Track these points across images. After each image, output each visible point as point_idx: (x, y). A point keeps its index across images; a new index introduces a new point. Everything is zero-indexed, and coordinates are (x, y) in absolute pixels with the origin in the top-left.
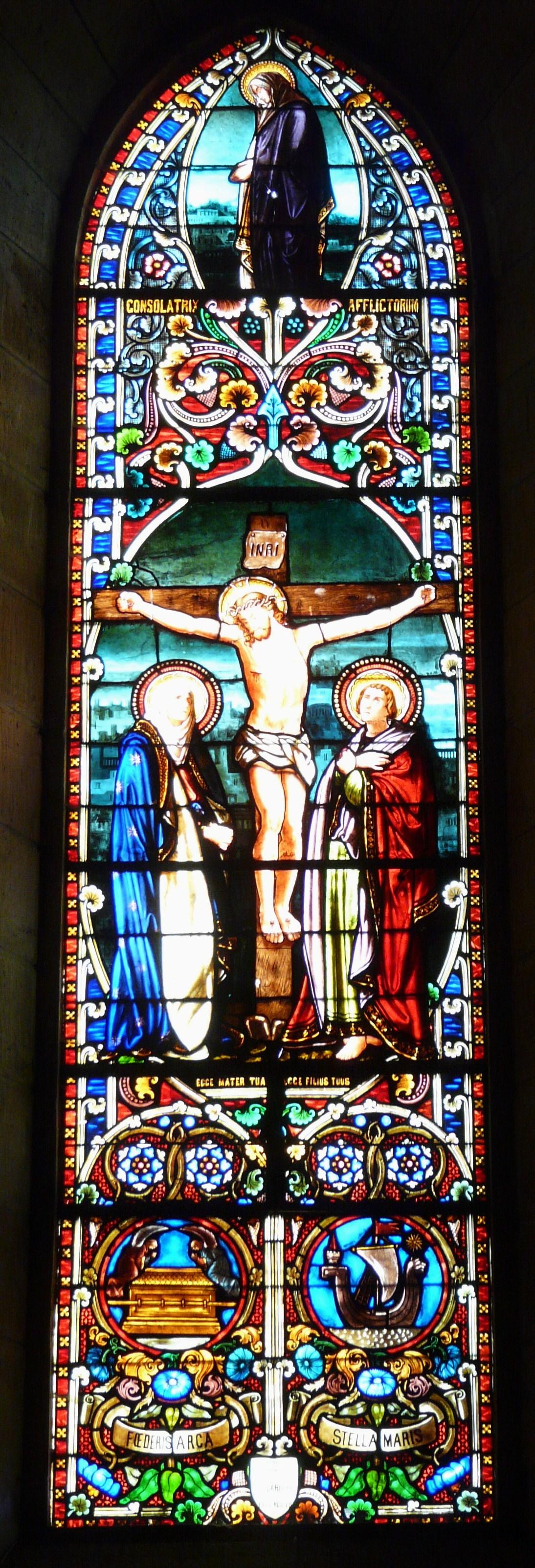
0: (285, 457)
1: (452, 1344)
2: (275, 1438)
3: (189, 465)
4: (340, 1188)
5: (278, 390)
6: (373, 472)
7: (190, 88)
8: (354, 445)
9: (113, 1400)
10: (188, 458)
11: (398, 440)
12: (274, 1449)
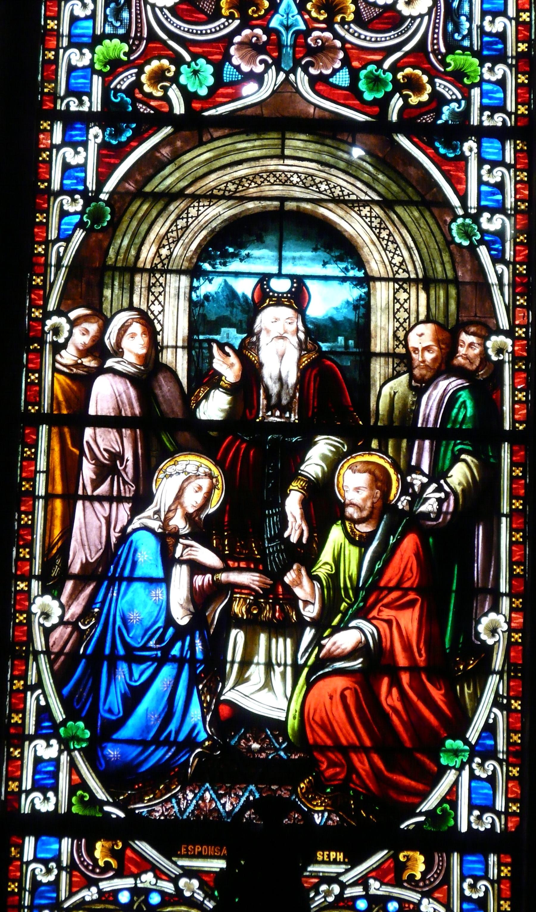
0: (301, 80)
3: (183, 89)
6: (406, 106)
10: (183, 80)
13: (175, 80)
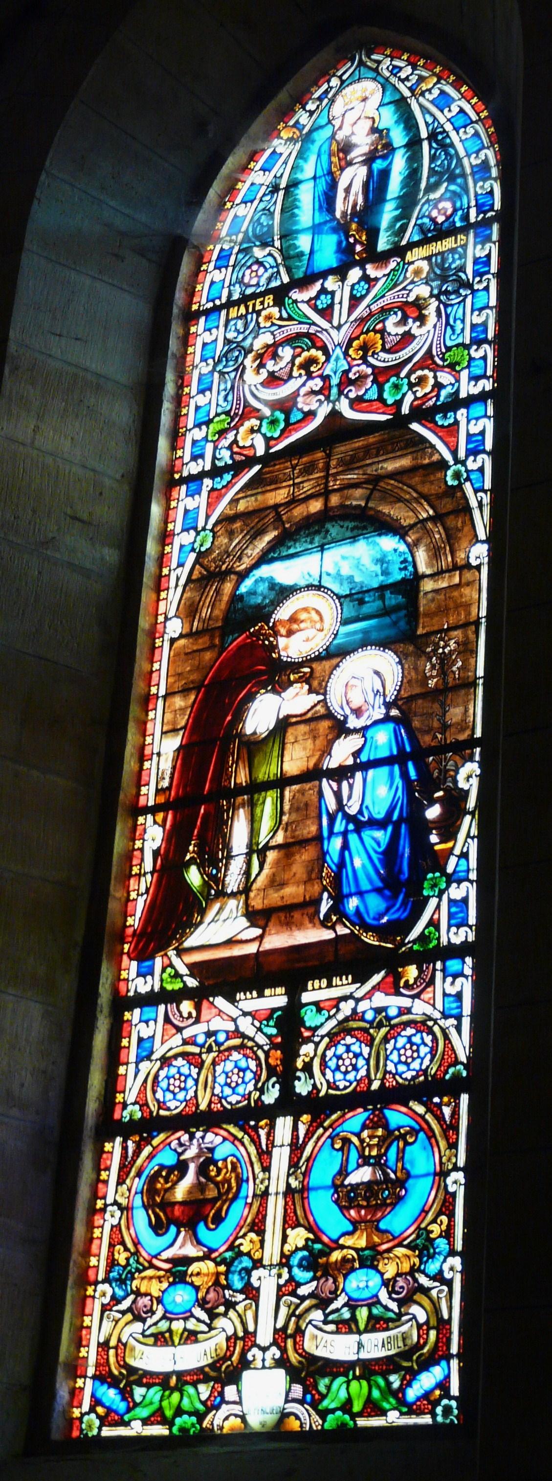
1: (440, 1236)
2: (264, 1349)
3: (264, 435)
4: (341, 1087)
5: (341, 348)
6: (416, 399)
7: (291, 123)
8: (402, 379)
9: (129, 1316)
11: (440, 363)
12: (264, 1360)
13: (259, 431)
